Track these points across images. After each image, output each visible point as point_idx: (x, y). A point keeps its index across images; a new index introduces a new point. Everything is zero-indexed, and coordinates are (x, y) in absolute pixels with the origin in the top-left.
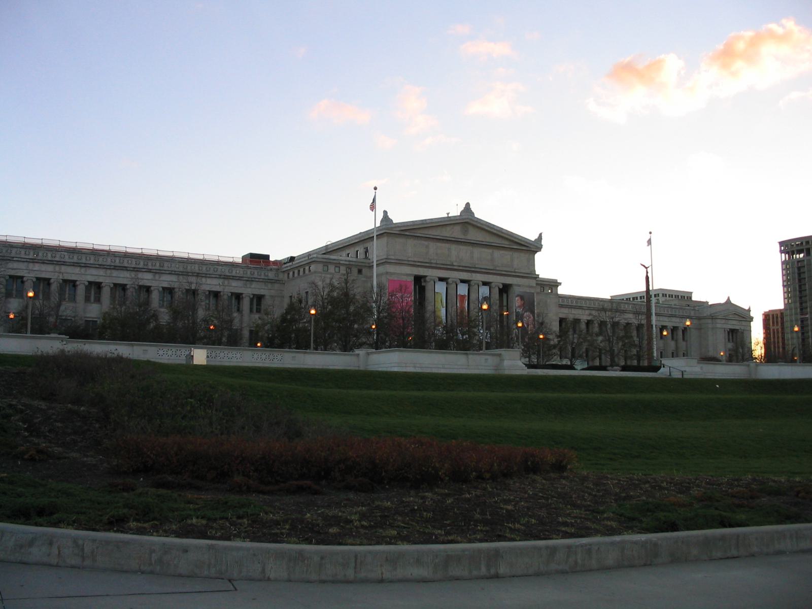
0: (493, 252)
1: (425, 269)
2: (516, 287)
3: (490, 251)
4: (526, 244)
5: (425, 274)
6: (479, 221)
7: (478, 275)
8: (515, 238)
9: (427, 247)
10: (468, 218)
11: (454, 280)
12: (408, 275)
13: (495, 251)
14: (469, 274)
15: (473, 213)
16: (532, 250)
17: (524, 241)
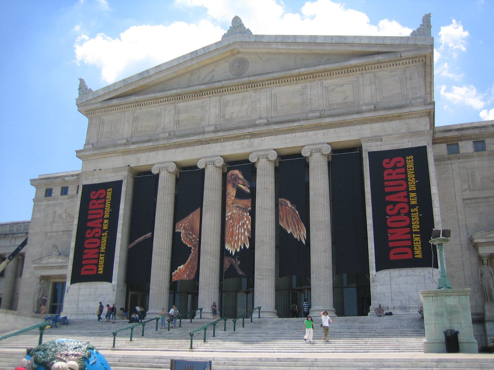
0: (305, 88)
1: (152, 154)
2: (368, 144)
3: (298, 87)
4: (386, 50)
5: (150, 163)
6: (260, 40)
7: (267, 139)
8: (352, 45)
9: (159, 115)
10: (234, 43)
11: (210, 159)
12: (116, 170)
13: (309, 84)
14: (246, 141)
15: (250, 31)
16: (404, 55)
17: (376, 45)
